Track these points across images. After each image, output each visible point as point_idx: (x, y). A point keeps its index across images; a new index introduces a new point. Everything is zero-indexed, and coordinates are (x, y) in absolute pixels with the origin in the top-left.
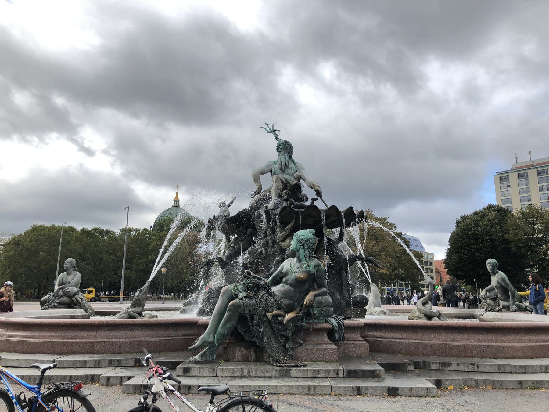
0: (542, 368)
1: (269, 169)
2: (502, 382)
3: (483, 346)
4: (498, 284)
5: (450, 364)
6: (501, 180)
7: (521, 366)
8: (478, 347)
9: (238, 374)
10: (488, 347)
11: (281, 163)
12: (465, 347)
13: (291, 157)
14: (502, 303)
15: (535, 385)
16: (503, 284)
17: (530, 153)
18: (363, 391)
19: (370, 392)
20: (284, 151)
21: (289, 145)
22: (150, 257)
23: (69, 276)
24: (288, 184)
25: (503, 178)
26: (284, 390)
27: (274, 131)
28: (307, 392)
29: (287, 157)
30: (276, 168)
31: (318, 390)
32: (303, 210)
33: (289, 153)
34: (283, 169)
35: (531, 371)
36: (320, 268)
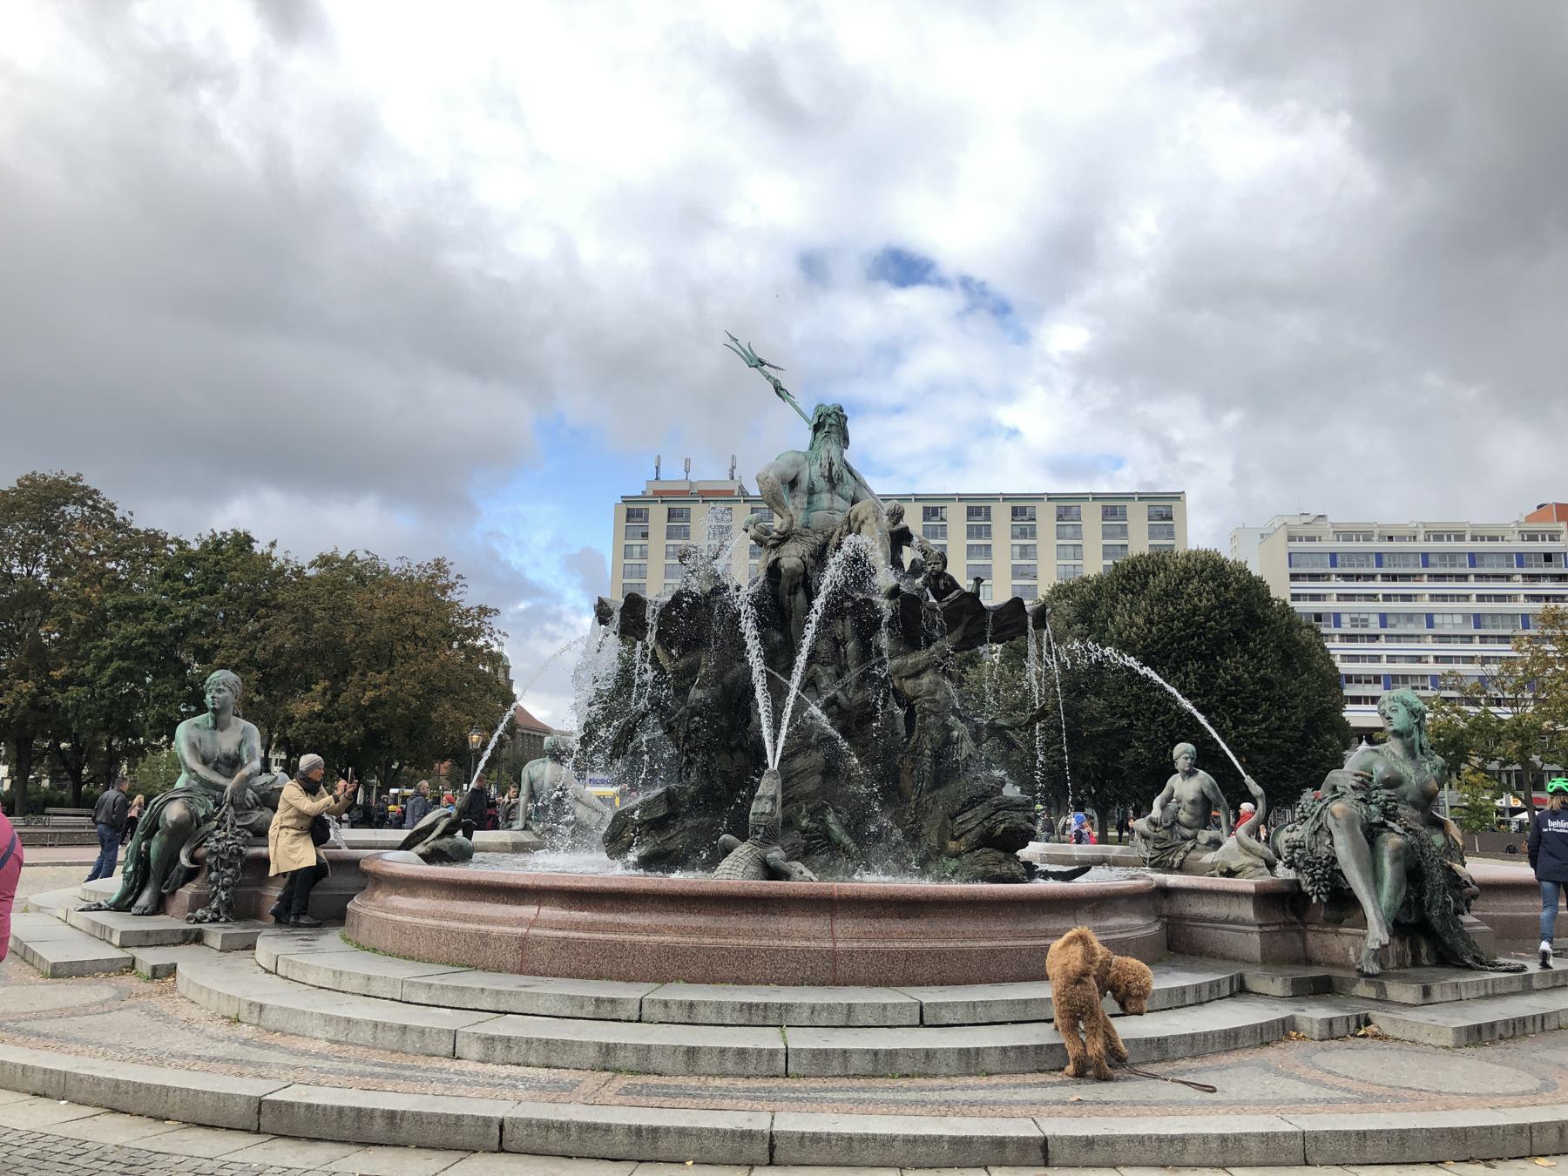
4: (1199, 796)
6: (631, 515)
11: (831, 465)
14: (1205, 836)
16: (1212, 796)
17: (687, 461)
23: (219, 734)
25: (634, 513)
27: (763, 363)
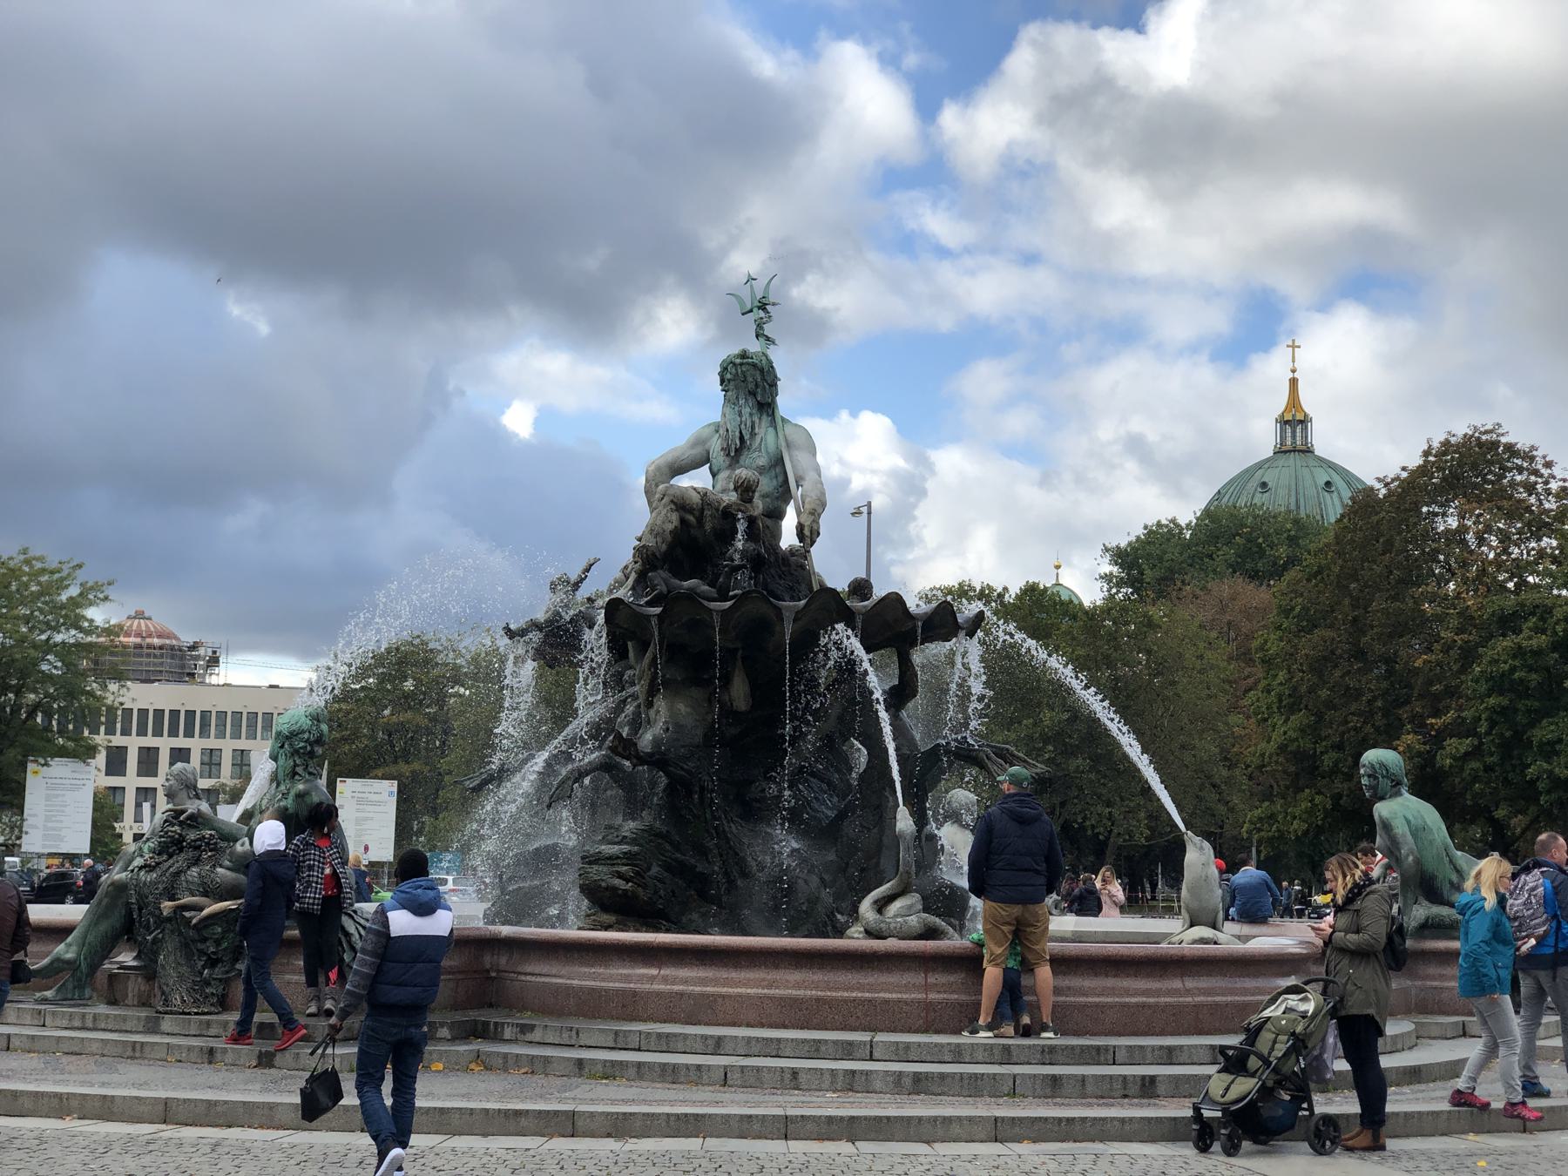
0: (709, 1042)
1: (697, 451)
2: (547, 1060)
3: (671, 994)
5: (532, 1028)
7: (659, 1035)
8: (659, 994)
9: (77, 1023)
10: (681, 994)
12: (634, 993)
13: (766, 407)
15: (609, 1071)
18: (218, 1056)
19: (229, 1058)
20: (737, 388)
21: (754, 365)
22: (1047, 716)
24: (707, 513)
26: (94, 1047)
28: (129, 1053)
29: (746, 411)
30: (716, 445)
31: (147, 1049)
32: (658, 610)
33: (753, 394)
34: (737, 450)
35: (680, 1046)
36: (308, 799)
